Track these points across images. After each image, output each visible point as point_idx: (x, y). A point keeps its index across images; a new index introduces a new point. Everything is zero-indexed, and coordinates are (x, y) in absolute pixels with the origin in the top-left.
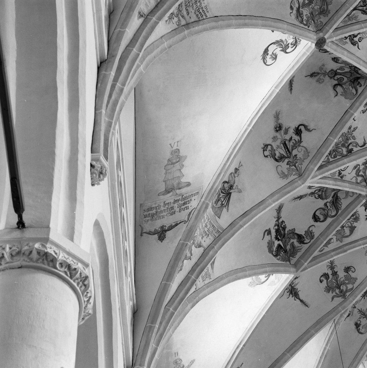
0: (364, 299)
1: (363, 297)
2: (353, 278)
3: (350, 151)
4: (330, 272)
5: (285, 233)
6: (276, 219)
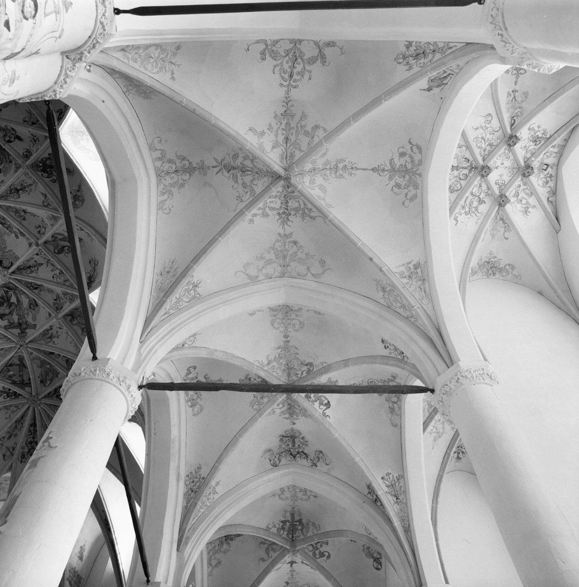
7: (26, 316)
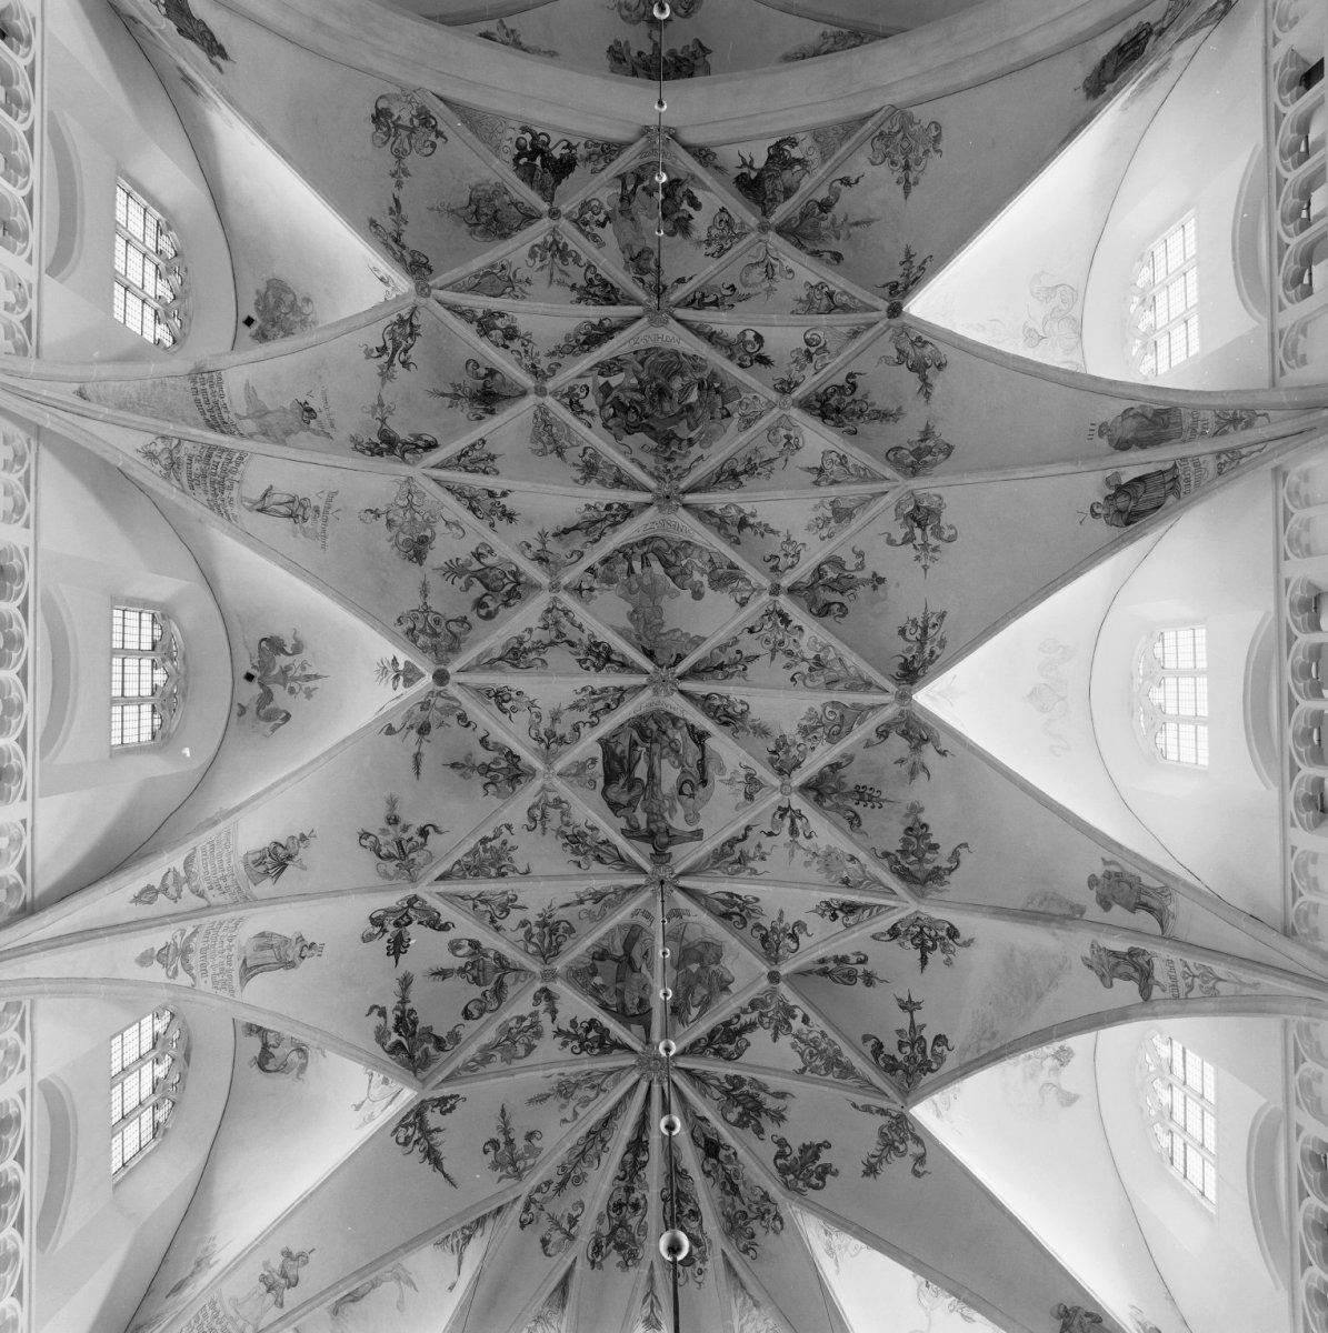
3: (503, 875)
4: (502, 1139)
5: (415, 1032)
6: (400, 999)
7: (666, 815)
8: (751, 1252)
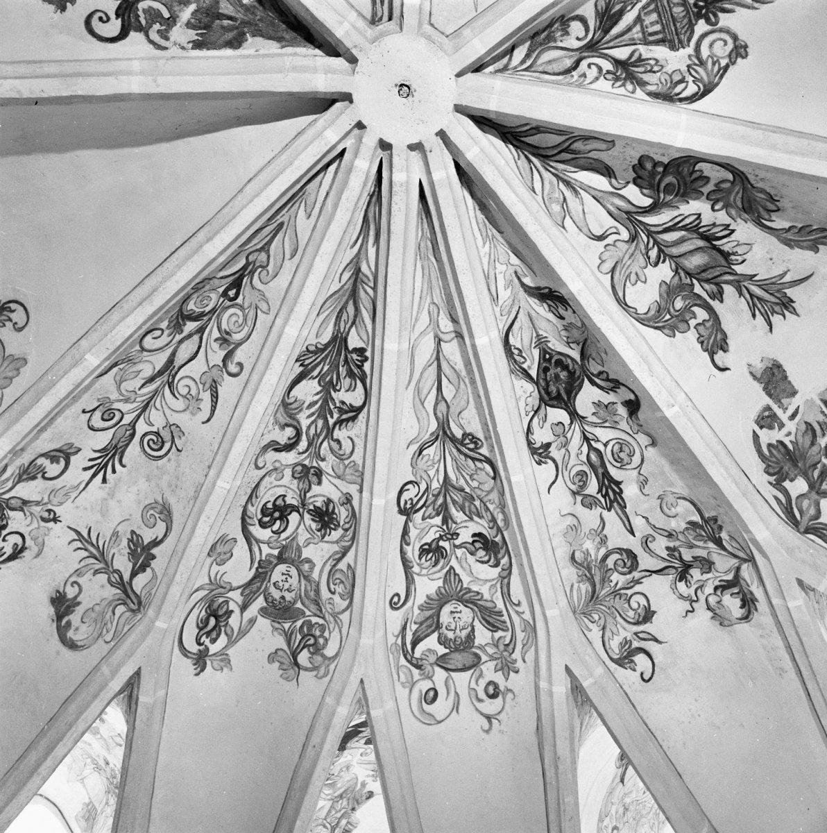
0: (104, 480)
1: (94, 475)
2: (14, 359)
8: (640, 659)
